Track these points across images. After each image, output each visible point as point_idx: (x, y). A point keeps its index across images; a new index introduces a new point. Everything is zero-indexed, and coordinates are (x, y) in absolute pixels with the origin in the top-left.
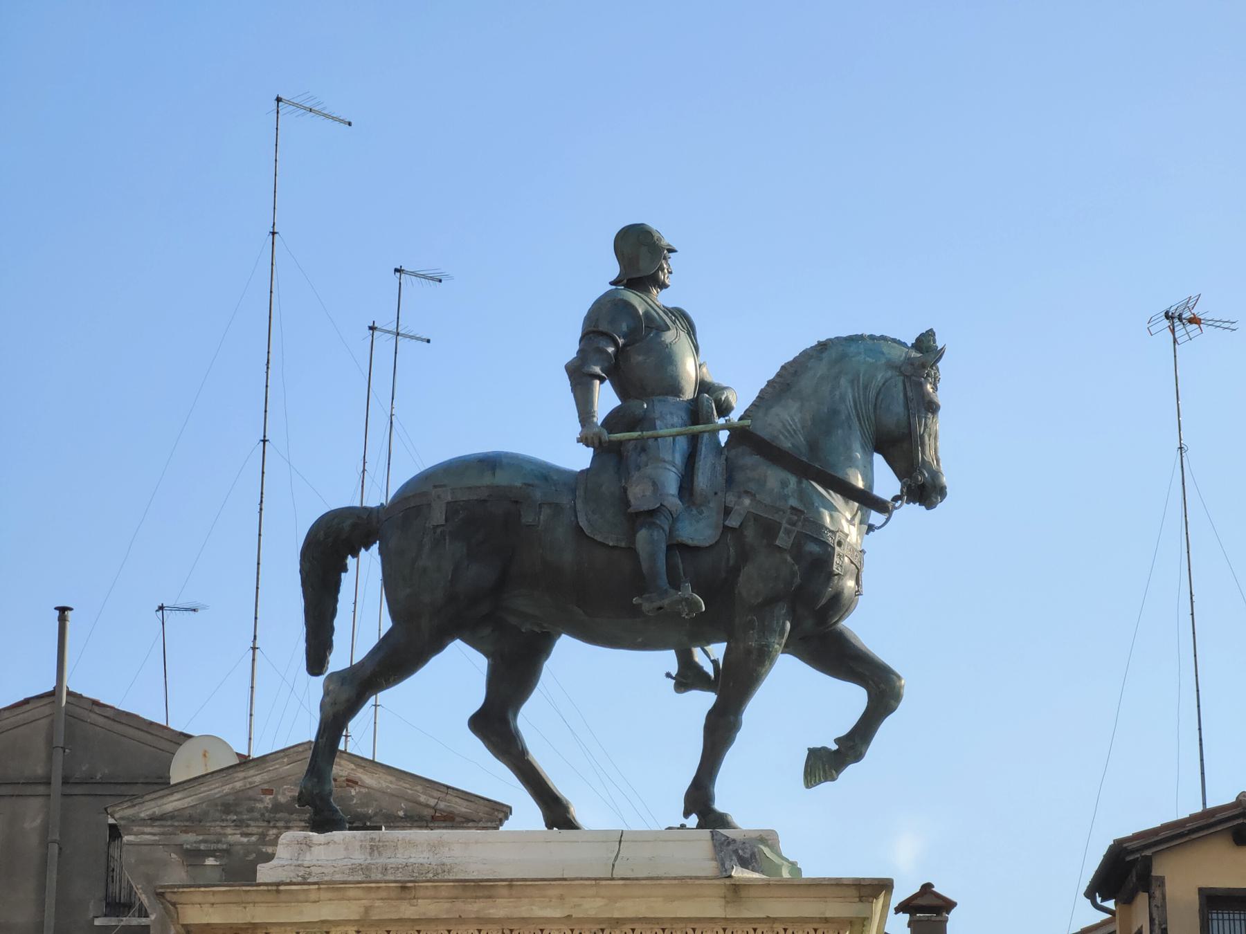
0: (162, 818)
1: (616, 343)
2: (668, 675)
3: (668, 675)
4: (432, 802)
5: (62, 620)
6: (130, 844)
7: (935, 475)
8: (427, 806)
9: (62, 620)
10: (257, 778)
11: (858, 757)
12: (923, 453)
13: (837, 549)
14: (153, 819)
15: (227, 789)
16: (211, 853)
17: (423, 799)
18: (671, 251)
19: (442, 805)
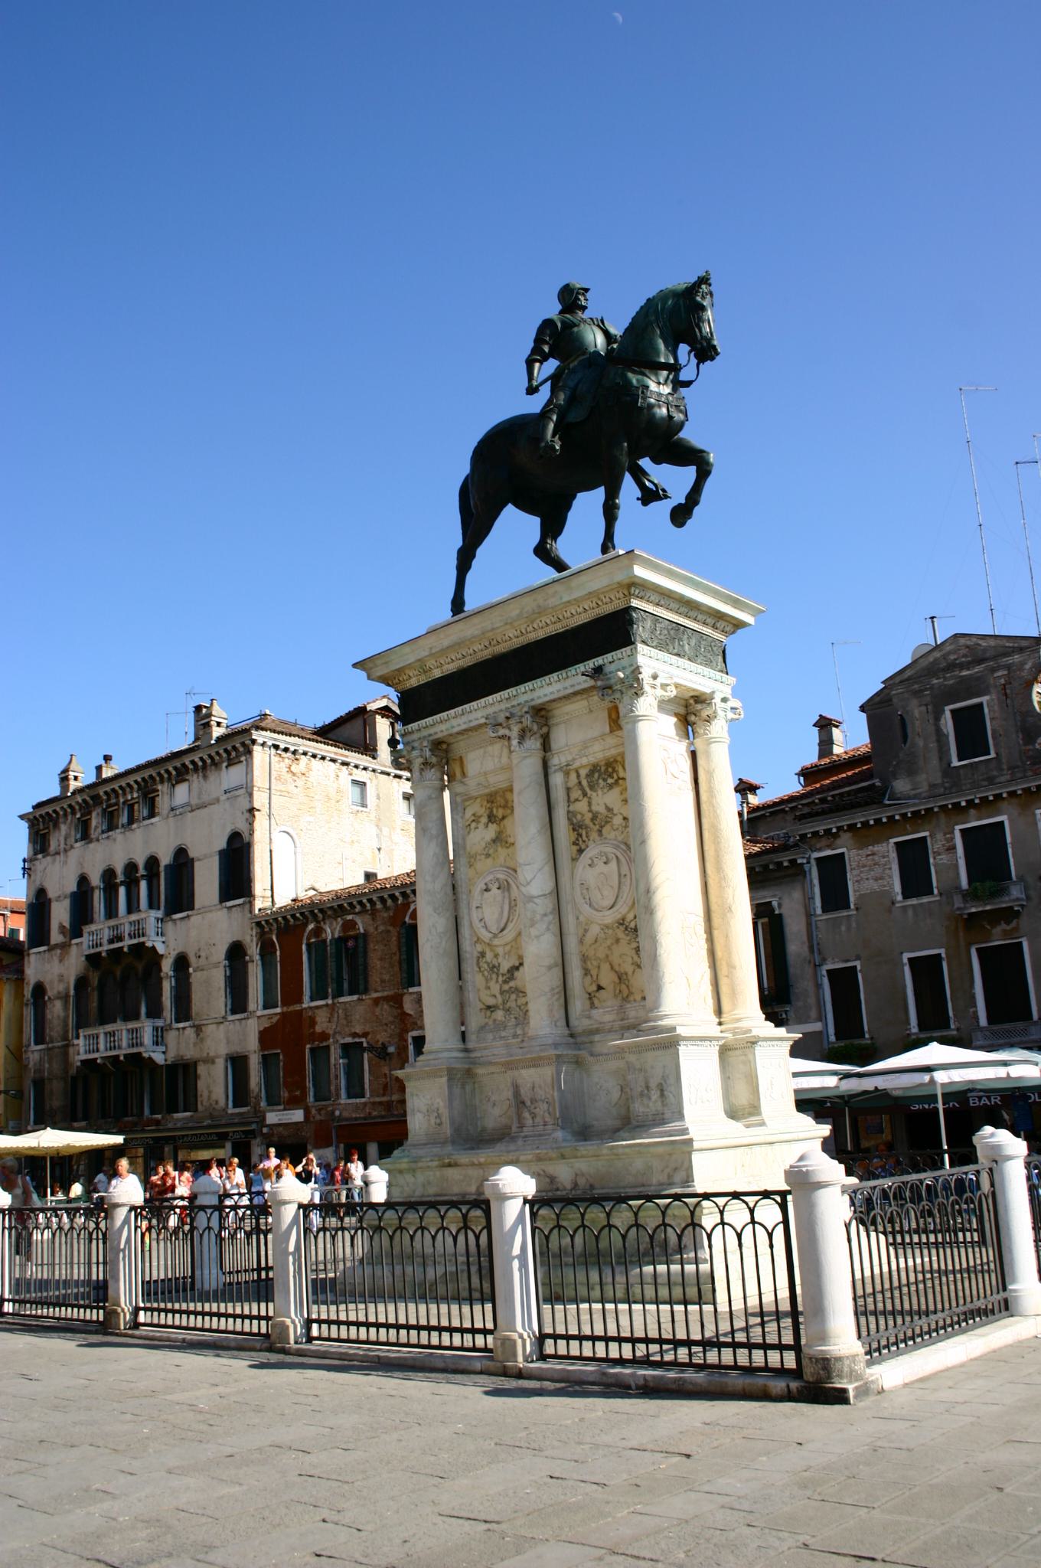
0: (907, 680)
1: (547, 343)
2: (638, 499)
3: (638, 499)
4: (1011, 645)
5: (933, 622)
6: (894, 695)
7: (709, 340)
8: (1009, 647)
9: (933, 622)
10: (937, 654)
11: (696, 503)
12: (701, 332)
13: (641, 395)
14: (901, 682)
15: (927, 663)
16: (926, 690)
17: (1007, 644)
18: (587, 290)
19: (1016, 645)
